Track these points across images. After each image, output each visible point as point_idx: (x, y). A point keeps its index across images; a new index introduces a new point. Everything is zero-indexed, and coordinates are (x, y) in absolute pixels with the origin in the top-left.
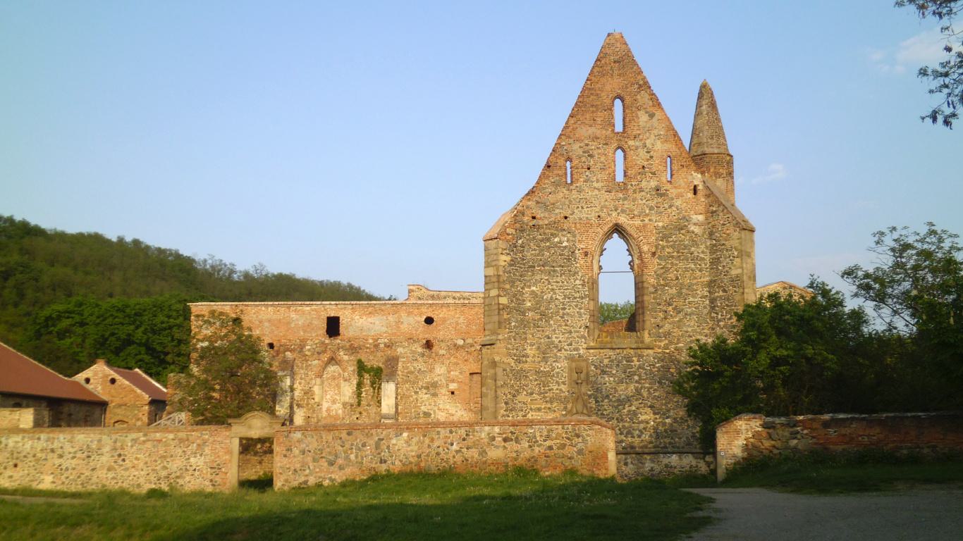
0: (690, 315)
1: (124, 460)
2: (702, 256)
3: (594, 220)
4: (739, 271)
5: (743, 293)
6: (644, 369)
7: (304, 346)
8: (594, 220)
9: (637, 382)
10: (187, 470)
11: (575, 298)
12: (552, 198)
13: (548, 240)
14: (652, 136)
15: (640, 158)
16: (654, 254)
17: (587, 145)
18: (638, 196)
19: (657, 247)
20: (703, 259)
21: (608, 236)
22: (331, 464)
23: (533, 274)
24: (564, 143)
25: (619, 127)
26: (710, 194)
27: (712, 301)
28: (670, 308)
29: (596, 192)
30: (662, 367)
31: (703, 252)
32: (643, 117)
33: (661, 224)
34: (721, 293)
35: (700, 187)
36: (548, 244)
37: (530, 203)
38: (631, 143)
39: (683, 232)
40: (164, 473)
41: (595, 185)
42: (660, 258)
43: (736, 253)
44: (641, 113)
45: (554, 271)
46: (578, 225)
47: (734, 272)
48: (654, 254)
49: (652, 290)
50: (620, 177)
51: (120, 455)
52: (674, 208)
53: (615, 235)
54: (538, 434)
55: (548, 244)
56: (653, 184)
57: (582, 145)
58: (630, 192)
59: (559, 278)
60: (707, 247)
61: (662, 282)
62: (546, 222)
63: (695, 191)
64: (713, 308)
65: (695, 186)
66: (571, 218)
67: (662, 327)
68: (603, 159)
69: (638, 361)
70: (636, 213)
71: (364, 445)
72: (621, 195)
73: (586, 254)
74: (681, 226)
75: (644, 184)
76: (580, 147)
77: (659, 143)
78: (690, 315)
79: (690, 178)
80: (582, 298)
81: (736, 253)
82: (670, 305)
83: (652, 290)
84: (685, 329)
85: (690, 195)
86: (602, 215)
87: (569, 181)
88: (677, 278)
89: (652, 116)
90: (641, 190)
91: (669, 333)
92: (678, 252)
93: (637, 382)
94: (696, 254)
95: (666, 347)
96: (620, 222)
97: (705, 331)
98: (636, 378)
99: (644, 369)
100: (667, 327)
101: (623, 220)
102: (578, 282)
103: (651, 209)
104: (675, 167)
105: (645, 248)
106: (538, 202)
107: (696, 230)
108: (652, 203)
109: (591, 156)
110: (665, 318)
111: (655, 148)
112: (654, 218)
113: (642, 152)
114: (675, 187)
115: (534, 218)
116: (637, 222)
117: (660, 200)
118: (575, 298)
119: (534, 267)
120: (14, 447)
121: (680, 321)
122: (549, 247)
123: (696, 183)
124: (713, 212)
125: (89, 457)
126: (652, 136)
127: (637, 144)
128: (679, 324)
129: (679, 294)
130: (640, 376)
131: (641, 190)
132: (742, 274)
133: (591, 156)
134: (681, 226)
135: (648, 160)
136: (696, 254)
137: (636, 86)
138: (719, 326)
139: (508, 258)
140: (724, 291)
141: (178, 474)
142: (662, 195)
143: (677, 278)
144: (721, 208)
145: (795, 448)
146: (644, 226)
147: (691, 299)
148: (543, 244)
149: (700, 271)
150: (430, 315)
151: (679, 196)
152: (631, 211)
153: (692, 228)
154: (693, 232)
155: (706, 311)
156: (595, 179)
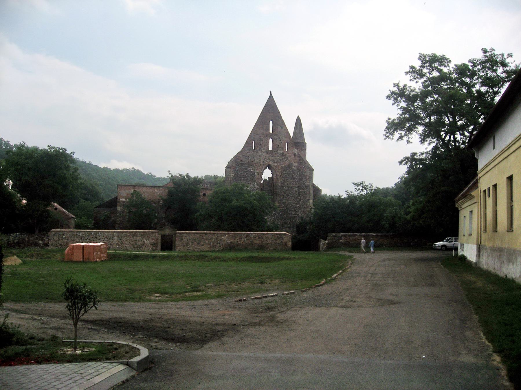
0: (291, 197)
1: (122, 241)
2: (296, 177)
3: (262, 163)
4: (309, 184)
5: (310, 191)
6: (276, 214)
7: (160, 202)
8: (262, 163)
9: (273, 219)
10: (144, 245)
11: (254, 189)
12: (248, 154)
13: (246, 169)
14: (282, 135)
15: (278, 142)
16: (281, 176)
17: (260, 136)
18: (276, 155)
19: (282, 173)
20: (297, 178)
21: (266, 168)
22: (199, 244)
23: (241, 180)
24: (252, 135)
25: (271, 131)
26: (300, 157)
27: (299, 193)
28: (285, 194)
29: (263, 153)
30: (282, 214)
31: (297, 176)
32: (279, 128)
33: (283, 166)
34: (302, 190)
35: (296, 154)
36: (246, 170)
37: (240, 155)
38: (275, 137)
39: (290, 169)
40: (136, 246)
41: (262, 150)
42: (283, 177)
43: (308, 178)
44: (278, 127)
45: (248, 180)
46: (256, 165)
47: (307, 184)
48: (281, 176)
49: (279, 188)
50: (270, 149)
51: (120, 240)
52: (288, 161)
53: (268, 168)
54: (269, 237)
55: (246, 170)
56: (281, 152)
57: (259, 136)
58: (274, 154)
59: (249, 182)
60: (298, 175)
61: (283, 185)
62: (246, 162)
63: (295, 155)
64: (299, 195)
65: (295, 154)
66: (254, 162)
67: (282, 201)
68: (265, 142)
69: (274, 212)
70: (275, 161)
71: (212, 238)
72: (271, 155)
73: (258, 174)
74: (290, 166)
75: (278, 151)
76: (258, 137)
77: (284, 138)
78: (291, 197)
79: (294, 151)
80: (257, 189)
81: (308, 178)
82: (285, 193)
83: (279, 188)
84: (290, 201)
85: (293, 156)
86: (264, 161)
87: (254, 149)
88: (288, 184)
89: (282, 128)
90: (277, 153)
91: (284, 203)
92: (289, 175)
93: (273, 219)
94: (294, 176)
95: (283, 207)
96: (270, 164)
97: (296, 203)
98: (273, 217)
99: (276, 214)
100: (284, 201)
101: (271, 163)
102: (255, 184)
103: (280, 160)
104: (289, 147)
105: (278, 174)
106: (243, 155)
107: (295, 168)
108: (281, 158)
109: (262, 140)
110: (284, 198)
111: (283, 139)
112: (281, 163)
113: (278, 140)
114: (289, 153)
115: (241, 161)
116: (276, 164)
117: (284, 157)
118: (254, 189)
119: (241, 178)
120: (82, 236)
121: (288, 198)
122: (246, 172)
123: (295, 152)
124: (300, 163)
125: (109, 240)
126: (282, 135)
127: (277, 137)
128: (287, 200)
129: (288, 190)
130: (274, 217)
131: (277, 153)
132: (310, 185)
133: (262, 140)
134: (290, 166)
135: (280, 143)
136: (294, 176)
137: (278, 117)
138: (300, 201)
139: (233, 175)
140: (303, 190)
141: (141, 246)
142: (284, 156)
143: (288, 184)
144: (303, 162)
145: (341, 242)
146: (278, 166)
147: (292, 192)
148: (244, 170)
149: (296, 182)
150: (205, 193)
151: (289, 156)
152: (274, 160)
153: (293, 168)
154: (294, 169)
155: (296, 196)
156: (262, 148)
